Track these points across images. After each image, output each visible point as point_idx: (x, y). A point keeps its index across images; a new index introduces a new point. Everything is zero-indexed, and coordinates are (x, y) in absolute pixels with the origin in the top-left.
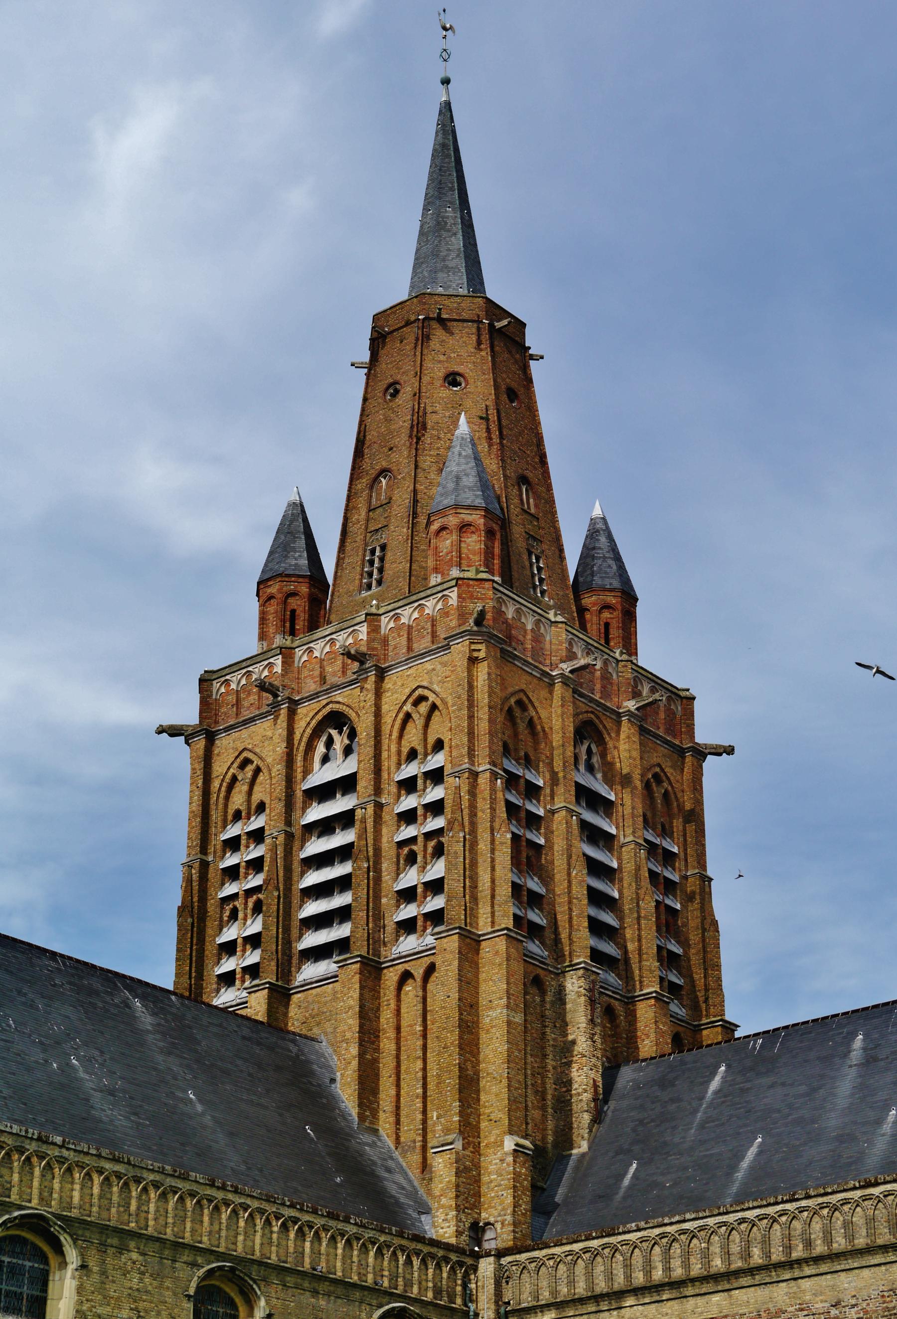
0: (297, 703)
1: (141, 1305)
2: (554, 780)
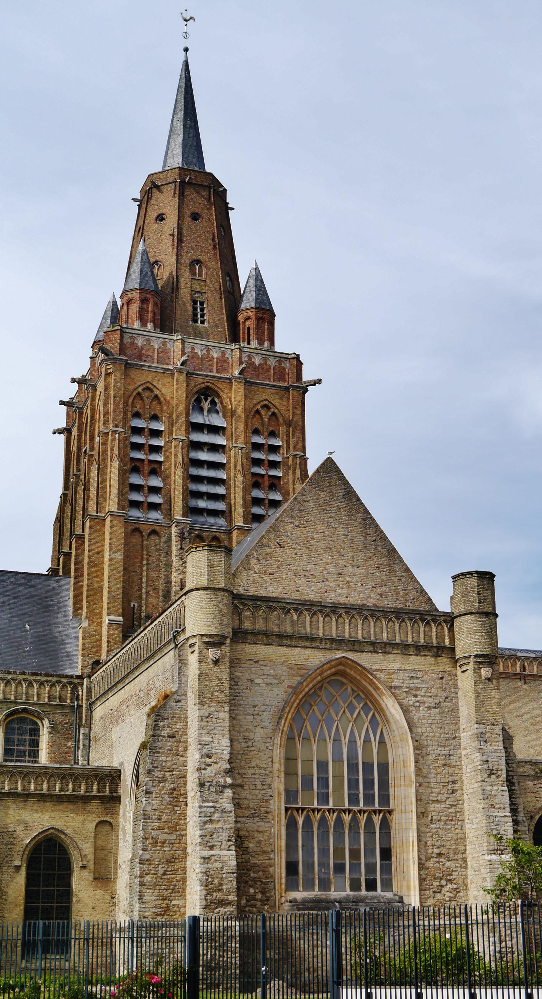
2: (172, 424)
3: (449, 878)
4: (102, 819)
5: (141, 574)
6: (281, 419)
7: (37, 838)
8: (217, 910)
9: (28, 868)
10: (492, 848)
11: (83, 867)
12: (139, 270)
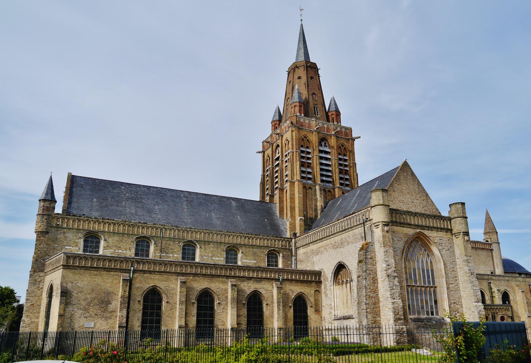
0: (273, 144)
1: (213, 253)
2: (314, 150)
3: (458, 311)
4: (316, 289)
5: (307, 203)
6: (347, 150)
7: (296, 296)
8: (398, 322)
9: (294, 307)
10: (475, 300)
11: (311, 307)
12: (297, 95)
